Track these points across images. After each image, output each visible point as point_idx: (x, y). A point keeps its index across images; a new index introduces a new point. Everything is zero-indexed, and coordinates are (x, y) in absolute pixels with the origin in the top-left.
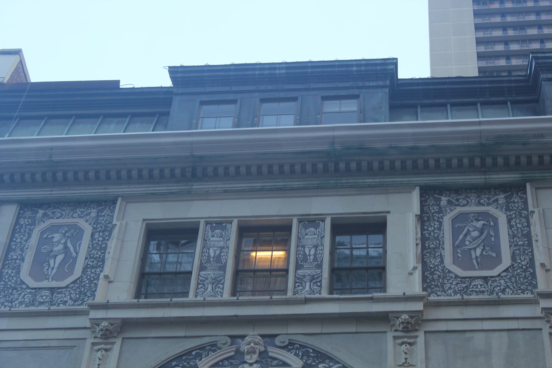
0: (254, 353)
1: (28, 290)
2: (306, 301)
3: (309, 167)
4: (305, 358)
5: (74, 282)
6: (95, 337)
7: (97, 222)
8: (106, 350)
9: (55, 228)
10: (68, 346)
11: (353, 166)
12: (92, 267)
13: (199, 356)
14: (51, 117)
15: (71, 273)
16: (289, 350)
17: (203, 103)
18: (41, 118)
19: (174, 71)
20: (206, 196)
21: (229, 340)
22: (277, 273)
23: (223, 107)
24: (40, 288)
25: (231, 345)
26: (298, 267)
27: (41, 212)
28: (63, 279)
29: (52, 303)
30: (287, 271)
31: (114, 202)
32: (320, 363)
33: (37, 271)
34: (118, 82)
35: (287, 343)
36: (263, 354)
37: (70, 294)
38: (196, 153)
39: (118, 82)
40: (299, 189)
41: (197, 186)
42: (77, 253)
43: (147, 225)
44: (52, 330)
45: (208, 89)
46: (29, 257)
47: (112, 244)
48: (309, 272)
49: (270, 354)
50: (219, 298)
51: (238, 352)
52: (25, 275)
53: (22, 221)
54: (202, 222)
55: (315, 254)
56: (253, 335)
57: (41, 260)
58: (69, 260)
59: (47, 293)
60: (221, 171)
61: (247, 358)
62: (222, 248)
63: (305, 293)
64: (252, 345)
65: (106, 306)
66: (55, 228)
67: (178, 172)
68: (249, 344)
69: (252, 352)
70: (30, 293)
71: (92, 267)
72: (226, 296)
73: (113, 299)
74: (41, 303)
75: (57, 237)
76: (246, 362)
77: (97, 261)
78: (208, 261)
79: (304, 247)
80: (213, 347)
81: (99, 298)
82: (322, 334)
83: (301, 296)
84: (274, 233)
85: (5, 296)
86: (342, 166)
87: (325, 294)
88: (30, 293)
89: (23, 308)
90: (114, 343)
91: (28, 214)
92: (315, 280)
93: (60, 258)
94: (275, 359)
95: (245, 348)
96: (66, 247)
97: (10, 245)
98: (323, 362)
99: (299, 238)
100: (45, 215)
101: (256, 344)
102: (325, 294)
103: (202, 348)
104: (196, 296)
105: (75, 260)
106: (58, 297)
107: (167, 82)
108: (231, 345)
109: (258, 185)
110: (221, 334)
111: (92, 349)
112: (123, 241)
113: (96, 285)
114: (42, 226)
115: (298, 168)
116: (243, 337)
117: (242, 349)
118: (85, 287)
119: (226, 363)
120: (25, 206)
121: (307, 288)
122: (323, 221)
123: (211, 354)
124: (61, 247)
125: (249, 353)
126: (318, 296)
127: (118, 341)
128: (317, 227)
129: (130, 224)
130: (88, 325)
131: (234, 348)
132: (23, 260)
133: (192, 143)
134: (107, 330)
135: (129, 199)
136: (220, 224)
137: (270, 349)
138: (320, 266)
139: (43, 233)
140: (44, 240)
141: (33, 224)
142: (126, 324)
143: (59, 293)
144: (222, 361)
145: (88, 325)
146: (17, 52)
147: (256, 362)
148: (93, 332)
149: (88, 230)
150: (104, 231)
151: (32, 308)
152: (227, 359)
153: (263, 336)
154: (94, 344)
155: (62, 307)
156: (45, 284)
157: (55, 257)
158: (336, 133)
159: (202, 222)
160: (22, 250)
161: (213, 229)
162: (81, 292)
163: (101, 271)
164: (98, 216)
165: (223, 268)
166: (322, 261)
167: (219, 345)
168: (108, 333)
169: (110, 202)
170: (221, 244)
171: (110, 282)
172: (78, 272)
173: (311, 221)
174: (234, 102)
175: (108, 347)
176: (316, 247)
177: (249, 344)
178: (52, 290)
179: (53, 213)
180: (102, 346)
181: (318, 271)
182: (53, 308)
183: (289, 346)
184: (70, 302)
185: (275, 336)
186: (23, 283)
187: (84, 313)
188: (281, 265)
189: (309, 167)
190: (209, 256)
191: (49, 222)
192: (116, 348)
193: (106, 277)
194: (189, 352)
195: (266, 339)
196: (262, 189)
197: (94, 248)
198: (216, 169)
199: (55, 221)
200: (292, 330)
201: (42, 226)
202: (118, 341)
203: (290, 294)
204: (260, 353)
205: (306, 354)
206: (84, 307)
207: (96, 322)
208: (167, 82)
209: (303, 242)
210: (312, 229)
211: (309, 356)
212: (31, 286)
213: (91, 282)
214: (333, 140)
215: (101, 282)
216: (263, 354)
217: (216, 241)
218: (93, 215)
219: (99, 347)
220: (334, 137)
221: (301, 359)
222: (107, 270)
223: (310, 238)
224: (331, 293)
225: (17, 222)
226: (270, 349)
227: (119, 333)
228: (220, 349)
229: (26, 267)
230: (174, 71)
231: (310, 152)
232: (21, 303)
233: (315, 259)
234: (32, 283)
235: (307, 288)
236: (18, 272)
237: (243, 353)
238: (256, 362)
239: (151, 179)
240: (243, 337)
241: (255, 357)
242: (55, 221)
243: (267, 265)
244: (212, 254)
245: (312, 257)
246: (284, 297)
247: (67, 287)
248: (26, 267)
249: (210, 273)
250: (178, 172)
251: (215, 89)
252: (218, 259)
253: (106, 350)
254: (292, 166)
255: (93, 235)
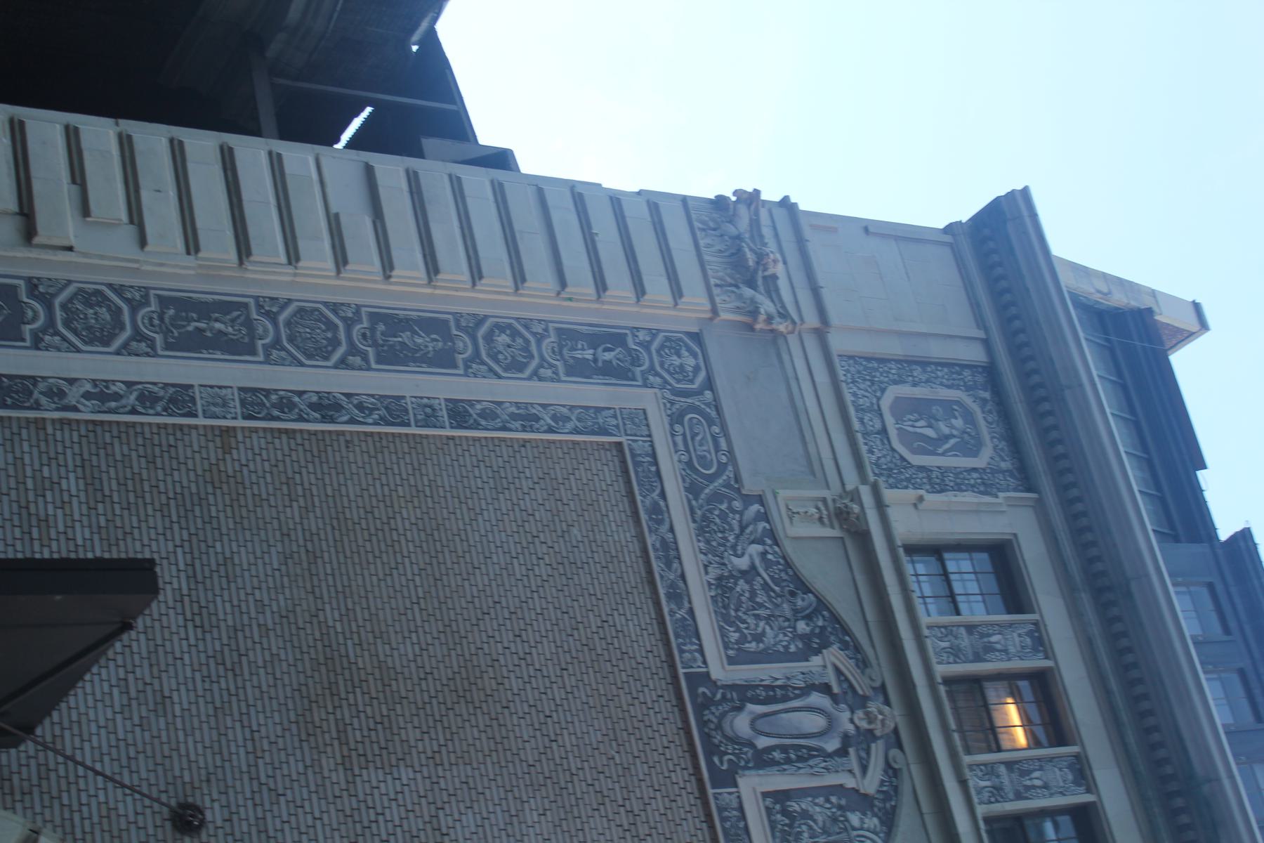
0: (870, 722)
1: (875, 401)
2: (963, 783)
3: (1161, 753)
4: (881, 796)
5: (903, 459)
6: (834, 500)
7: (993, 472)
8: (821, 519)
9: (969, 417)
10: (812, 469)
11: (1184, 819)
12: (930, 478)
13: (845, 646)
14: (1124, 388)
15: (915, 452)
16: (885, 771)
17: (1211, 587)
18: (1120, 374)
19: (1244, 538)
20: (1075, 613)
21: (877, 684)
22: (991, 735)
23: (1214, 618)
24: (881, 415)
25: (873, 688)
26: (1009, 765)
27: (987, 395)
28: (903, 442)
29: (866, 434)
30: (999, 750)
31: (1029, 489)
32: (879, 818)
33: (904, 408)
34: (1204, 467)
35: (896, 766)
36: (870, 736)
37: (884, 456)
38: (1134, 587)
39: (1204, 467)
40: (1125, 745)
41: (1085, 598)
42: (943, 454)
43: (1009, 541)
44: (830, 443)
45: (1233, 590)
46: (920, 392)
47: (969, 498)
48: (1006, 780)
49: (873, 745)
50: (934, 660)
51: (863, 701)
52: (893, 392)
53: (967, 373)
54: (1035, 617)
55: (1034, 787)
56: (893, 716)
57: (920, 408)
58: (931, 446)
59: (878, 426)
60: (1118, 627)
61: (860, 713)
62: (1006, 651)
63: (974, 782)
64: (880, 717)
65: (881, 506)
66: (969, 417)
67: (1099, 566)
68: (881, 713)
69: (870, 718)
70: (872, 404)
71: (930, 478)
72: (940, 670)
73: (893, 514)
74: (861, 420)
75: (959, 423)
76: (852, 712)
77: (940, 482)
78: (982, 636)
79: (1041, 769)
80: (863, 664)
81: (889, 495)
82: (921, 814)
83: (968, 774)
84: (1052, 723)
85: (859, 372)
86: (1179, 802)
87: (981, 810)
88: (872, 404)
89: (849, 398)
90: (832, 527)
91: (980, 379)
92: (997, 793)
93: (930, 433)
94: (868, 753)
95: (873, 707)
96: (948, 437)
97: (929, 363)
98: (882, 822)
99: (1051, 759)
100: (984, 401)
101: (883, 721)
102: (981, 810)
103: (857, 648)
104: (929, 627)
105: (934, 453)
106: (876, 441)
107: (1225, 531)
108: (873, 688)
109: (1113, 684)
110: (883, 671)
111: (818, 499)
112: (977, 512)
113: (906, 487)
114: (968, 400)
115: (1156, 737)
116: (887, 702)
117: (870, 704)
118: (900, 474)
119: (845, 685)
120: (990, 372)
121: (983, 784)
122: (1088, 791)
123: (852, 662)
124: (946, 431)
125: (867, 714)
126: (976, 800)
127: (836, 533)
128: (1076, 783)
129: (1007, 517)
130: (849, 487)
131: (869, 693)
132: (915, 385)
133: (1147, 575)
134: (848, 513)
135: (1040, 508)
136: (1040, 641)
137: (880, 743)
138: (1019, 796)
139: (958, 403)
140: (949, 408)
141: (968, 389)
142: (862, 537)
143: (883, 444)
144: (847, 679)
145: (849, 487)
146: (1204, 326)
147: (857, 727)
148: (841, 497)
149: (981, 461)
150: (987, 487)
151: (852, 411)
152: (851, 686)
153: (896, 731)
154: (824, 500)
155: (864, 449)
156: (890, 421)
157: (930, 426)
158: (1227, 783)
159: (1035, 617)
160: (927, 381)
161: (1029, 634)
162: (890, 469)
163: (928, 491)
164: (1003, 472)
165: (978, 658)
166: (1027, 798)
167: (868, 671)
168: (845, 515)
169: (1026, 481)
170: (1012, 650)
171: (915, 505)
172: (917, 460)
173: (1081, 772)
174: (1227, 630)
175: (826, 520)
176: (1046, 786)
177: (881, 713)
178: (884, 431)
179: (990, 412)
180: (825, 512)
181: (1011, 796)
182: (859, 436)
183: (891, 771)
184: (874, 458)
185: (900, 747)
186: (883, 390)
187: (864, 480)
188: (1005, 744)
189: (1161, 753)
190: (989, 635)
191: (975, 408)
192: (828, 532)
193: (921, 499)
194: (846, 631)
195: (893, 736)
196: (1108, 692)
197: (957, 475)
198: (1118, 619)
199: (979, 416)
200: (916, 770)
201: (968, 400)
202: (836, 533)
203: (967, 759)
204: (871, 731)
205: (887, 797)
206: (872, 478)
207: (855, 496)
208: (1225, 531)
209: (1048, 766)
210: (1070, 777)
211: (884, 801)
212: (882, 402)
213: (908, 480)
214: (1215, 780)
215: (911, 494)
216: (870, 736)
217: (1015, 640)
218: (1003, 465)
219: (823, 508)
220: (1218, 779)
221: (878, 791)
222: (931, 498)
223: (1059, 776)
224: (987, 820)
225: (964, 366)
226: (880, 743)
227: (848, 531)
228: (863, 673)
229: (905, 390)
230: (1244, 538)
231: (1185, 750)
232: (854, 394)
233: (1028, 788)
234: (886, 403)
235: (983, 784)
236: (895, 382)
237: (864, 706)
238: (857, 727)
239: (1077, 533)
240: (887, 702)
241: (864, 725)
242: (979, 416)
243: (998, 722)
244: (994, 639)
245: (1028, 783)
246: (960, 749)
247: (893, 450)
248: (905, 390)
249: (965, 641)
250: (1099, 566)
251: (1237, 600)
252: (989, 648)
253: (821, 519)
254: (1156, 729)
255: (975, 470)
